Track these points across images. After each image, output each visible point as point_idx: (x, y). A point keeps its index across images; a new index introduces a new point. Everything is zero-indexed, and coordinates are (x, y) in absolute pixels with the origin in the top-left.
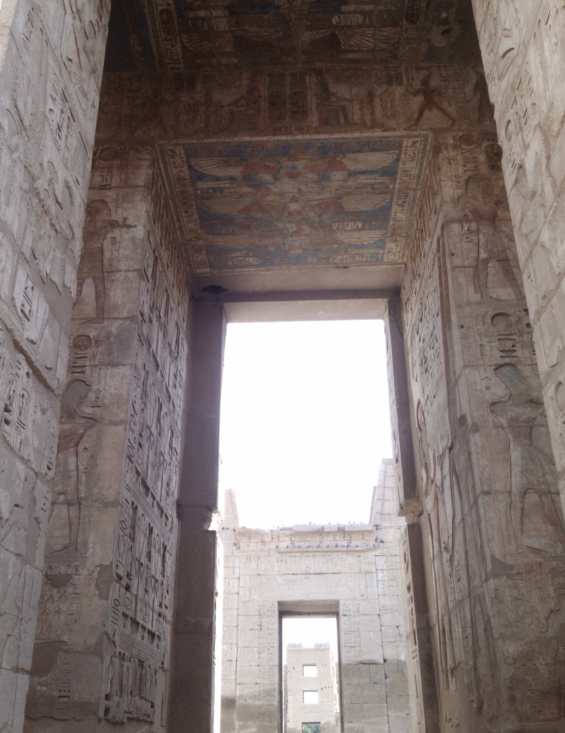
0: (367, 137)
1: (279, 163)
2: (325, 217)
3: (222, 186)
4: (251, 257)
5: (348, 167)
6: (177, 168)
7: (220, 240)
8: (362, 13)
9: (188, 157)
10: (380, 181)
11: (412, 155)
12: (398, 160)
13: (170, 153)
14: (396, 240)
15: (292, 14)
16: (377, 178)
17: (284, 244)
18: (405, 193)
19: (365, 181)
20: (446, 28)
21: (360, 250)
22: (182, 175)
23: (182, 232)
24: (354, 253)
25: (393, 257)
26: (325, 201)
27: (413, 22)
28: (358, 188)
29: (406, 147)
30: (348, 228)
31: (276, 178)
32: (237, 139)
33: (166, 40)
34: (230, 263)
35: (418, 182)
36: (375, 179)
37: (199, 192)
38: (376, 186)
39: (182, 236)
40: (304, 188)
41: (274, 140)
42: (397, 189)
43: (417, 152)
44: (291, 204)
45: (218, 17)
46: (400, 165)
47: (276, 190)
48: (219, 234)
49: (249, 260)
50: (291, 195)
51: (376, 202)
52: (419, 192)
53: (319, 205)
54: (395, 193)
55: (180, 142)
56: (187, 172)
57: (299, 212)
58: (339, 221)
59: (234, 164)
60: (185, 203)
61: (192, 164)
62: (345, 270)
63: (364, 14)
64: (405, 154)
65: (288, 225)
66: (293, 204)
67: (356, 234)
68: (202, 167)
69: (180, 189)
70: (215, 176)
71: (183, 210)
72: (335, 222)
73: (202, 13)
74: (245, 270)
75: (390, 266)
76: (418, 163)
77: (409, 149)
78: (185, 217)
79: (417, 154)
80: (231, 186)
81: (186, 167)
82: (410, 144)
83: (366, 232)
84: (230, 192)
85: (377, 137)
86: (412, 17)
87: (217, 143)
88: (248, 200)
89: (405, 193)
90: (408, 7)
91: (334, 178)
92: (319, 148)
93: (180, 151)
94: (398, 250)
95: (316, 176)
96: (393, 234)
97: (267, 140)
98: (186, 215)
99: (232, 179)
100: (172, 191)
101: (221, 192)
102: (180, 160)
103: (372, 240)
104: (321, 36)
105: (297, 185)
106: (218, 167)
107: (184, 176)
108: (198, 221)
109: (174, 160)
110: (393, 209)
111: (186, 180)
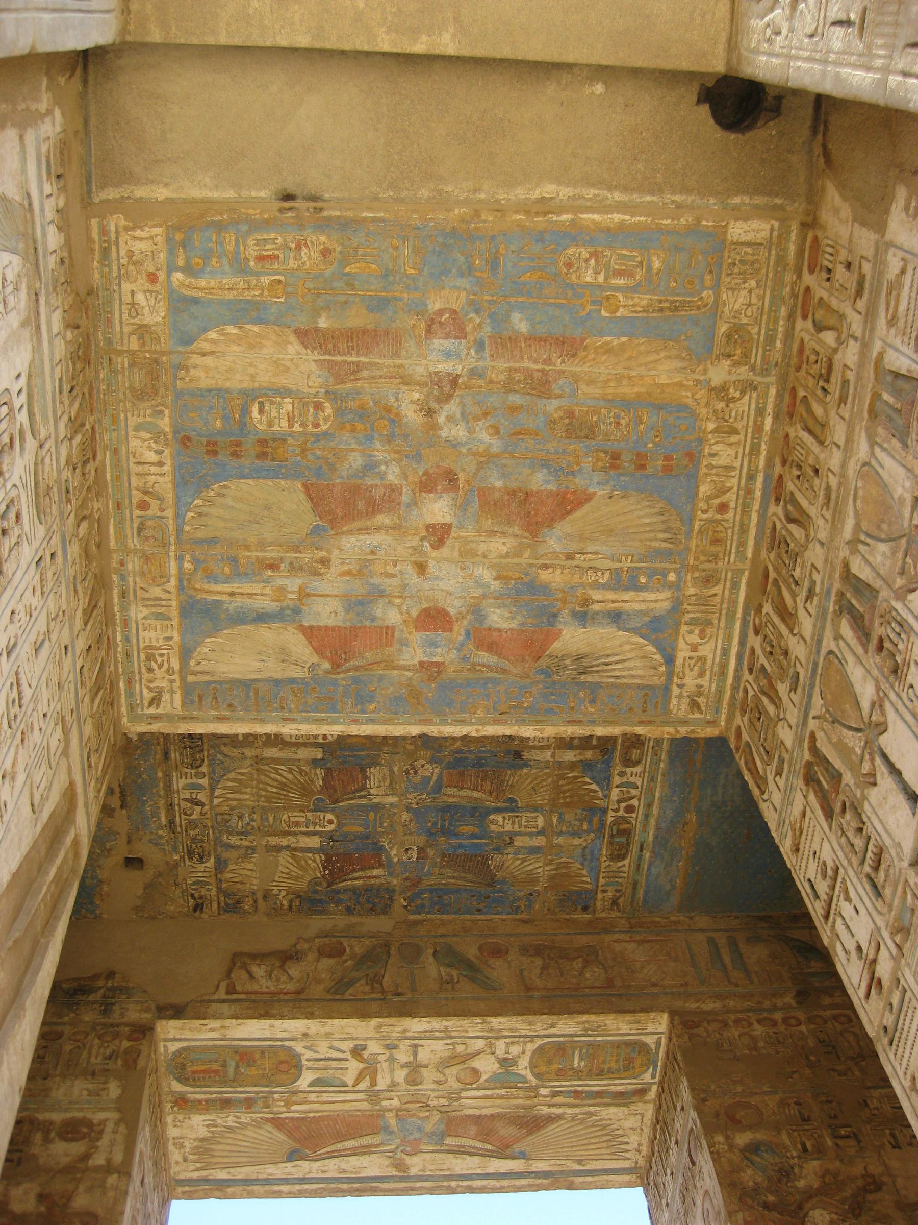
0: (262, 721)
1: (464, 659)
2: (356, 460)
3: (610, 596)
4: (589, 285)
5: (301, 637)
6: (700, 658)
7: (664, 380)
9: (667, 689)
10: (219, 587)
11: (154, 666)
12: (186, 653)
13: (701, 700)
14: (141, 337)
15: (412, 747)
16: (226, 598)
17: (480, 346)
18: (147, 538)
19: (256, 588)
21: (248, 296)
22: (694, 638)
23: (759, 428)
24: (265, 280)
25: (138, 246)
28: (273, 567)
29: (172, 692)
30: (288, 405)
31: (476, 611)
32: (550, 731)
34: (657, 264)
35: (123, 578)
36: (232, 594)
37: (672, 577)
38: (227, 570)
39: (760, 412)
40: (412, 577)
41: (473, 724)
42: (172, 554)
43: (146, 676)
44: (448, 519)
46: (176, 636)
48: (660, 407)
49: (597, 273)
50: (445, 551)
52: (112, 544)
53: (374, 508)
54: (172, 539)
55: (671, 730)
56: (681, 644)
57: (427, 485)
58: (318, 437)
59: (568, 662)
60: (716, 541)
61: (663, 669)
62: (292, 189)
64: (170, 671)
65: (459, 432)
66: (441, 520)
67: (265, 377)
68: (645, 657)
69: (712, 592)
70: (619, 629)
71: (730, 515)
72: (326, 434)
74: (617, 217)
75: (141, 192)
76: (135, 641)
77: (164, 684)
78: (732, 488)
79: (143, 670)
80: (590, 592)
81: (679, 661)
82: (166, 697)
83: (237, 382)
85: (242, 720)
87: (593, 722)
89: (147, 538)
90: (202, 751)
91: (335, 604)
93: (678, 706)
94: (126, 287)
95: (379, 613)
96: (153, 368)
97: (483, 724)
98: (724, 499)
99: (583, 617)
100: (735, 586)
101: (617, 572)
103: (214, 342)
105: (426, 585)
106: (608, 656)
107: (691, 632)
108: (704, 470)
109: (699, 681)
110: (168, 479)
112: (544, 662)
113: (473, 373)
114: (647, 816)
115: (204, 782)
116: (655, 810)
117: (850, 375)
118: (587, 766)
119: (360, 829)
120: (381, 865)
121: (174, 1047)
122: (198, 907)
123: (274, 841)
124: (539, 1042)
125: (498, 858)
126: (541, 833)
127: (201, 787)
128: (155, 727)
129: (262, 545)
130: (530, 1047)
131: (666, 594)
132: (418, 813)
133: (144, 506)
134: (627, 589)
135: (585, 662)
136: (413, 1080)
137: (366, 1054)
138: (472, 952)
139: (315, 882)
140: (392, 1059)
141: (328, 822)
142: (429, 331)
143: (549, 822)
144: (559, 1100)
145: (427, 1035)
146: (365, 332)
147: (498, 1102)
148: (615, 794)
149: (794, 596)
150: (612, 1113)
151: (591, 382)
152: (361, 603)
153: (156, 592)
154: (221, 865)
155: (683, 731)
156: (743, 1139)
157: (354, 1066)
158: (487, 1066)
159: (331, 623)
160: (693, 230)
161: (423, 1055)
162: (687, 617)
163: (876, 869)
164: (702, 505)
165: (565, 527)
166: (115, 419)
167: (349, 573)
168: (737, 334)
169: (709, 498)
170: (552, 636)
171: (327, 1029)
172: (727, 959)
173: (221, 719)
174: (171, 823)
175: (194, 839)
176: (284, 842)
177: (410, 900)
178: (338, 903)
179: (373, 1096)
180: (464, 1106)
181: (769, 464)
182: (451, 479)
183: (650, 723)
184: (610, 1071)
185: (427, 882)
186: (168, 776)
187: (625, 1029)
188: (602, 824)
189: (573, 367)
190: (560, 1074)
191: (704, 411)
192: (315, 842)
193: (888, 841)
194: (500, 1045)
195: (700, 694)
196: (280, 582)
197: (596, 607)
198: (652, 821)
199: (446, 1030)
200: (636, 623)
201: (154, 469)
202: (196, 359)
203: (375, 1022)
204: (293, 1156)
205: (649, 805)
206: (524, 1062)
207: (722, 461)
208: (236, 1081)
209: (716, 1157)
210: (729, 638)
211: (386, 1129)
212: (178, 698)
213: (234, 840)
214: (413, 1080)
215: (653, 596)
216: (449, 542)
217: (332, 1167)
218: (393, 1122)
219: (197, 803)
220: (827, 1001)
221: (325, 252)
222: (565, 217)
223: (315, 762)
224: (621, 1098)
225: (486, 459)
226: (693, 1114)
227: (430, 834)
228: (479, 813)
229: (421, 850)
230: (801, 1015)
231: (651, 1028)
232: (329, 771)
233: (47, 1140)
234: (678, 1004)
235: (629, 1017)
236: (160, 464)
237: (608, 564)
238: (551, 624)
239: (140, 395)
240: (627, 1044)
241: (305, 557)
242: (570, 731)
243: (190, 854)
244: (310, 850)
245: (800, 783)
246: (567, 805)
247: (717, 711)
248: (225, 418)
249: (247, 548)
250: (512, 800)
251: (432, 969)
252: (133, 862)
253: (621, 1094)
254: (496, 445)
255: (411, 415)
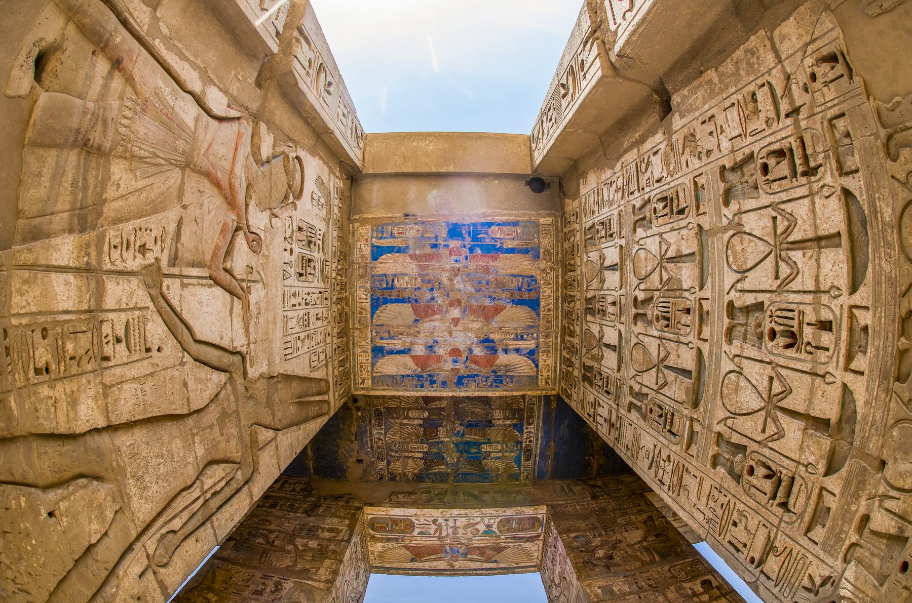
0: (398, 391)
2: (428, 296)
3: (515, 342)
7: (525, 267)
8: (410, 418)
9: (537, 377)
10: (384, 341)
12: (373, 365)
13: (549, 381)
14: (362, 259)
20: (356, 404)
22: (544, 357)
23: (557, 282)
24: (400, 239)
25: (363, 231)
26: (429, 319)
27: (378, 410)
28: (401, 334)
31: (471, 351)
33: (534, 404)
34: (519, 231)
35: (353, 338)
36: (388, 344)
37: (535, 335)
38: (387, 335)
39: (557, 277)
44: (459, 316)
45: (498, 419)
47: (470, 334)
48: (524, 277)
49: (501, 234)
50: (458, 328)
51: (385, 315)
53: (434, 313)
56: (540, 360)
57: (451, 304)
60: (548, 322)
63: (408, 418)
64: (367, 372)
65: (461, 286)
67: (399, 271)
71: (552, 312)
72: (419, 288)
73: (508, 422)
75: (364, 216)
77: (366, 376)
81: (540, 367)
82: (366, 381)
83: (391, 272)
84: (509, 333)
85: (391, 390)
86: (378, 414)
87: (512, 390)
88: (494, 324)
91: (422, 347)
92: (435, 382)
93: (542, 384)
94: (359, 243)
95: (437, 350)
99: (506, 351)
100: (556, 338)
102: (544, 373)
103: (384, 259)
104: (435, 403)
105: (452, 340)
108: (541, 297)
110: (369, 304)
111: (543, 351)
112: (494, 368)
113: (464, 267)
114: (537, 444)
115: (383, 432)
116: (539, 442)
117: (579, 243)
118: (515, 426)
119: (436, 451)
120: (444, 464)
121: (370, 517)
122: (381, 478)
123: (407, 454)
124: (500, 518)
125: (485, 461)
126: (500, 451)
127: (381, 434)
128: (363, 392)
129: (398, 326)
130: (497, 520)
131: (534, 342)
132: (457, 445)
133: (361, 313)
134: (520, 340)
135: (508, 368)
136: (455, 533)
137: (437, 523)
138: (477, 493)
139: (421, 470)
140: (447, 525)
141: (425, 447)
142: (450, 254)
143: (502, 447)
144: (508, 540)
145: (459, 516)
146: (430, 255)
147: (486, 541)
148: (525, 435)
149: (573, 325)
150: (527, 545)
151: (502, 269)
152: (431, 347)
153: (364, 343)
154: (389, 463)
155: (544, 392)
156: (572, 535)
157: (434, 527)
158: (482, 528)
159: (421, 353)
160: (530, 221)
161: (458, 523)
162: (541, 350)
163: (607, 387)
164: (542, 309)
165: (497, 318)
166: (354, 285)
167: (427, 336)
168: (547, 252)
169: (544, 307)
170: (495, 359)
171: (423, 513)
172: (567, 491)
173: (384, 390)
174: (372, 446)
175: (379, 453)
176: (410, 455)
177: (454, 477)
178: (430, 478)
179: (441, 538)
180: (473, 544)
181: (562, 293)
182: (459, 302)
183: (532, 390)
184: (526, 529)
185: (461, 471)
186: (371, 429)
187: (531, 512)
188: (521, 447)
189: (496, 264)
190: (509, 530)
191: (539, 277)
192: (420, 455)
193: (609, 372)
194: (486, 519)
195: (548, 378)
196: (404, 339)
197: (510, 347)
198: (539, 446)
199: (466, 514)
200: (524, 352)
201: (365, 301)
202: (379, 265)
203: (440, 510)
204: (412, 560)
205: (537, 440)
206: (495, 526)
207: (547, 294)
208: (392, 531)
209: (563, 540)
210: (556, 357)
211: (446, 552)
212: (370, 381)
213: (393, 454)
214: (455, 533)
215: (529, 343)
216: (459, 324)
217: (427, 565)
218: (448, 549)
219: (380, 439)
220: (602, 498)
221: (418, 231)
222: (490, 218)
223: (420, 425)
224: (531, 539)
225: (471, 296)
226: (556, 531)
227: (461, 453)
228: (478, 444)
229: (458, 459)
230: (593, 502)
231: (540, 512)
232: (425, 429)
233: (323, 531)
234: (550, 503)
235: (532, 508)
236: (367, 299)
237: (513, 331)
238: (495, 353)
239: (361, 277)
240: (532, 518)
241: (412, 331)
242: (505, 394)
243: (378, 458)
244: (419, 458)
245: (582, 383)
246: (508, 440)
247: (555, 385)
248: (387, 284)
249: (393, 327)
250: (489, 439)
251: (462, 497)
252: (359, 461)
253: (530, 537)
254: (473, 291)
255: (445, 281)
